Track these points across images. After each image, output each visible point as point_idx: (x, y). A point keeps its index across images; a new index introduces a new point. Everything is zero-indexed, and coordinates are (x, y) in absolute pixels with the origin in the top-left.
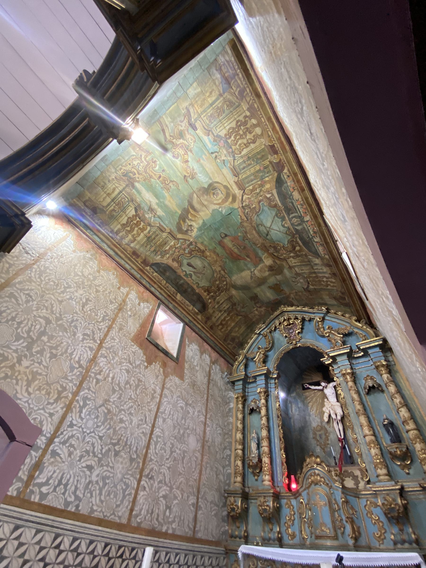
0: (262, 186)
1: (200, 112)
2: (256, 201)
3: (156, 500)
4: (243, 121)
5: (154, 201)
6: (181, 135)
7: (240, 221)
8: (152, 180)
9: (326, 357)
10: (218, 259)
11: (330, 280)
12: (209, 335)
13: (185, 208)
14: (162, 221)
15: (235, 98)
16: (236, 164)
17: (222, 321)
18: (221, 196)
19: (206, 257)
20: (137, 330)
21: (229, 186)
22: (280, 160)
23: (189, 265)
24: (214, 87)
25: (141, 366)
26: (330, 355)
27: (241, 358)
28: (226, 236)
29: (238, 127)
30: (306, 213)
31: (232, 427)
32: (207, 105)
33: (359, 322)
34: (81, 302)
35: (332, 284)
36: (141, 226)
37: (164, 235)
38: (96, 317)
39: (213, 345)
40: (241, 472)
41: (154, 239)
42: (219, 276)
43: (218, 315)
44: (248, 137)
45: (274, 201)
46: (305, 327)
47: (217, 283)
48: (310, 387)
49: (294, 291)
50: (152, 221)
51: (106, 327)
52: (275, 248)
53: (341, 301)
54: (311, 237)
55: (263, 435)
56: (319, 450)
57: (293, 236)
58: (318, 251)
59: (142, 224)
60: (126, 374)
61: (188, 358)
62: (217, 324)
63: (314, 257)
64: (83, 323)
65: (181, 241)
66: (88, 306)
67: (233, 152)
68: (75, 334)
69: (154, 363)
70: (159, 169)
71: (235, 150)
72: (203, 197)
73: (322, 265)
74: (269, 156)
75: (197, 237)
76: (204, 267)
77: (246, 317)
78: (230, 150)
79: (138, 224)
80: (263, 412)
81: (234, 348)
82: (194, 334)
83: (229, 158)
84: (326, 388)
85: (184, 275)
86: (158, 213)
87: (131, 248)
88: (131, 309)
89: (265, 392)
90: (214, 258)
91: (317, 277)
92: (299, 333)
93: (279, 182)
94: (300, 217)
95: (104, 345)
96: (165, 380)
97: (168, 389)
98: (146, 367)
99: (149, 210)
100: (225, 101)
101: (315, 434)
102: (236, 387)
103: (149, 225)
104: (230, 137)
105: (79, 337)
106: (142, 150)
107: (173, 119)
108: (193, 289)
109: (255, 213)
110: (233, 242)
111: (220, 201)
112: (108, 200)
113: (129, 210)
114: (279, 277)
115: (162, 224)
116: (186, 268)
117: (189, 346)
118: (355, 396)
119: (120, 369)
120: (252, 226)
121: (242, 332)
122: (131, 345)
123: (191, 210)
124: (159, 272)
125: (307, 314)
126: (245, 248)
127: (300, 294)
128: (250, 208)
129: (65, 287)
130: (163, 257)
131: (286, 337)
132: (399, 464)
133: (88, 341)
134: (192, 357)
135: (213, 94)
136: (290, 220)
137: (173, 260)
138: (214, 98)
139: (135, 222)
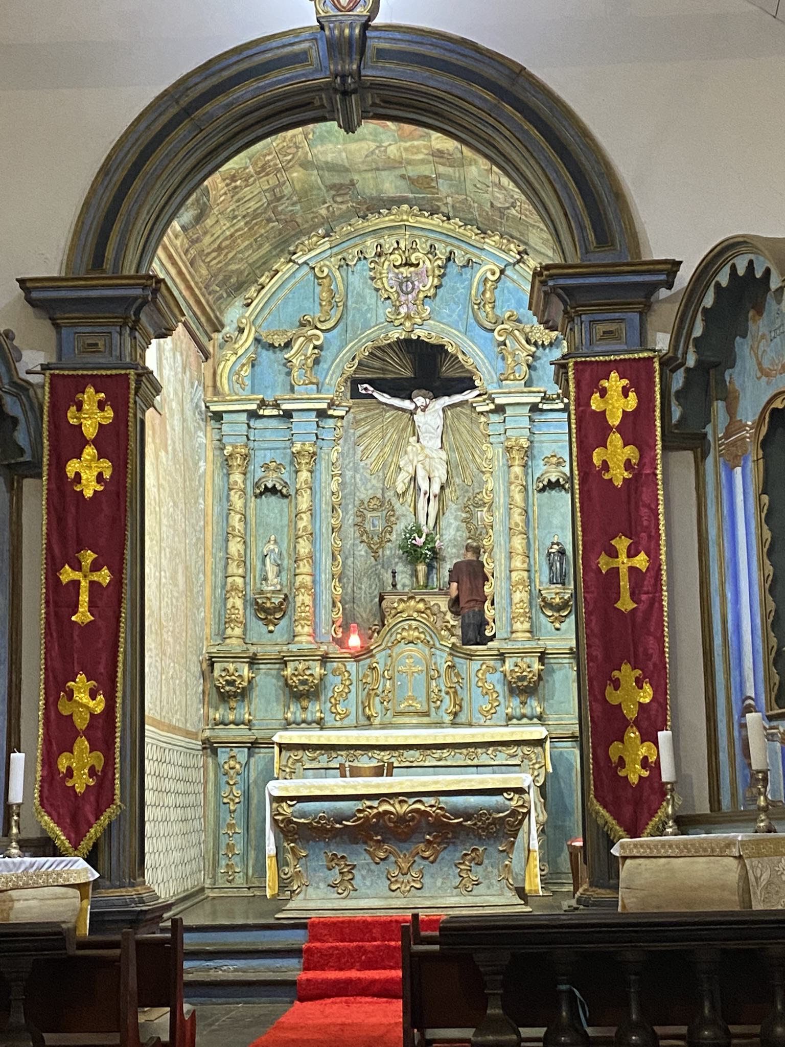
3: (169, 684)
17: (226, 239)
26: (497, 401)
31: (206, 523)
40: (241, 619)
47: (268, 158)
48: (375, 394)
55: (302, 551)
56: (363, 553)
62: (209, 250)
80: (304, 502)
81: (221, 297)
84: (423, 410)
89: (314, 454)
101: (363, 517)
102: (224, 427)
118: (518, 498)
121: (255, 258)
125: (463, 245)
131: (389, 298)
132: (550, 614)
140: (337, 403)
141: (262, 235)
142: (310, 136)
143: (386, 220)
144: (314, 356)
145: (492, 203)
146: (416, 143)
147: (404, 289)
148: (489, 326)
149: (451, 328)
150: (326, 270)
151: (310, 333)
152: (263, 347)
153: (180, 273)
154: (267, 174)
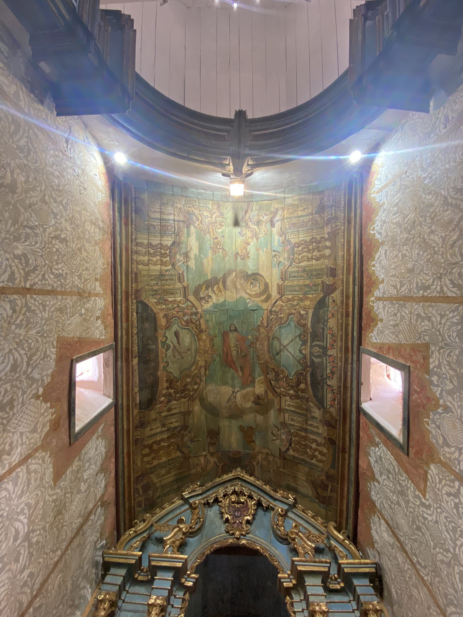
0: (301, 300)
1: (285, 217)
2: (287, 311)
4: (319, 240)
5: (194, 252)
6: (258, 223)
7: (259, 323)
8: (208, 235)
9: (289, 572)
10: (209, 351)
11: (320, 448)
12: (125, 451)
13: (216, 277)
14: (187, 272)
15: (322, 222)
16: (290, 270)
18: (257, 289)
19: (199, 340)
20: (73, 337)
21: (270, 286)
22: (334, 284)
23: (176, 334)
24: (310, 207)
25: (35, 385)
26: (299, 568)
27: (141, 526)
28: (236, 330)
29: (311, 242)
30: (333, 345)
32: (295, 215)
33: (339, 532)
34: (59, 232)
35: (319, 457)
36: (164, 260)
37: (179, 285)
38: (55, 264)
39: (120, 473)
41: (166, 280)
42: (196, 371)
43: (157, 428)
44: (314, 254)
45: (305, 320)
46: (257, 517)
47: (189, 380)
49: (266, 451)
50: (179, 264)
51: (52, 286)
52: (277, 374)
53: (320, 491)
54: (325, 376)
57: (304, 369)
58: (325, 397)
59: (168, 259)
60: (8, 368)
61: (86, 454)
62: (146, 443)
63: (316, 405)
64: (38, 245)
65: (189, 303)
66: (60, 244)
67: (293, 259)
68: (17, 239)
69: (49, 404)
70: (220, 233)
71: (296, 258)
72: (241, 279)
73: (321, 420)
74: (325, 277)
75: (207, 311)
76: (189, 350)
77: (186, 458)
78: (292, 257)
79: (162, 255)
82: (113, 428)
83: (286, 262)
85: (162, 342)
86: (189, 263)
87: (137, 268)
88: (87, 310)
90: (206, 346)
91: (305, 438)
92: (248, 522)
93: (321, 304)
94: (325, 349)
95: (28, 296)
96: (36, 450)
97: (29, 472)
98: (37, 397)
99: (184, 254)
100: (312, 219)
103: (173, 265)
104: (299, 247)
105: (17, 248)
106: (219, 211)
107: (260, 209)
108: (156, 368)
109: (279, 323)
110: (238, 341)
111: (254, 293)
112: (158, 216)
113: (167, 239)
114: (260, 418)
115: (185, 274)
116: (170, 334)
117: (97, 438)
119: (10, 351)
120: (268, 336)
121: (166, 482)
122: (52, 342)
123: (221, 283)
124: (139, 315)
126: (245, 356)
127: (271, 458)
128: (277, 315)
129: (61, 202)
130: (158, 303)
131: (227, 520)
133: (20, 266)
134: (89, 460)
135: (306, 210)
136: (311, 347)
137: (165, 316)
138: (304, 214)
139: (163, 252)
140: (189, 572)
141: (172, 459)
142: (207, 372)
143: (230, 476)
144: (181, 540)
145: (280, 449)
146: (249, 389)
147: (236, 514)
148: (284, 537)
149: (262, 539)
150: (197, 502)
151: (182, 526)
152: (152, 543)
153: (128, 430)
154: (185, 397)
